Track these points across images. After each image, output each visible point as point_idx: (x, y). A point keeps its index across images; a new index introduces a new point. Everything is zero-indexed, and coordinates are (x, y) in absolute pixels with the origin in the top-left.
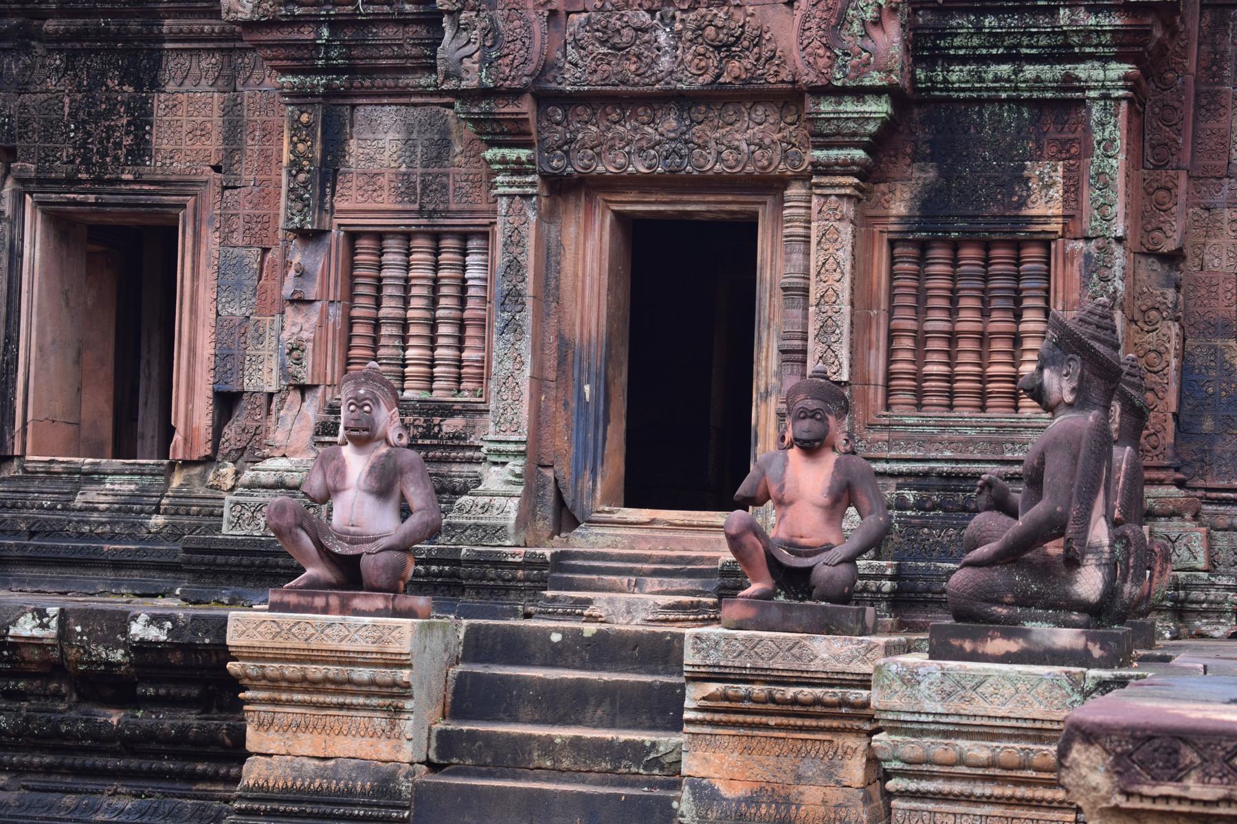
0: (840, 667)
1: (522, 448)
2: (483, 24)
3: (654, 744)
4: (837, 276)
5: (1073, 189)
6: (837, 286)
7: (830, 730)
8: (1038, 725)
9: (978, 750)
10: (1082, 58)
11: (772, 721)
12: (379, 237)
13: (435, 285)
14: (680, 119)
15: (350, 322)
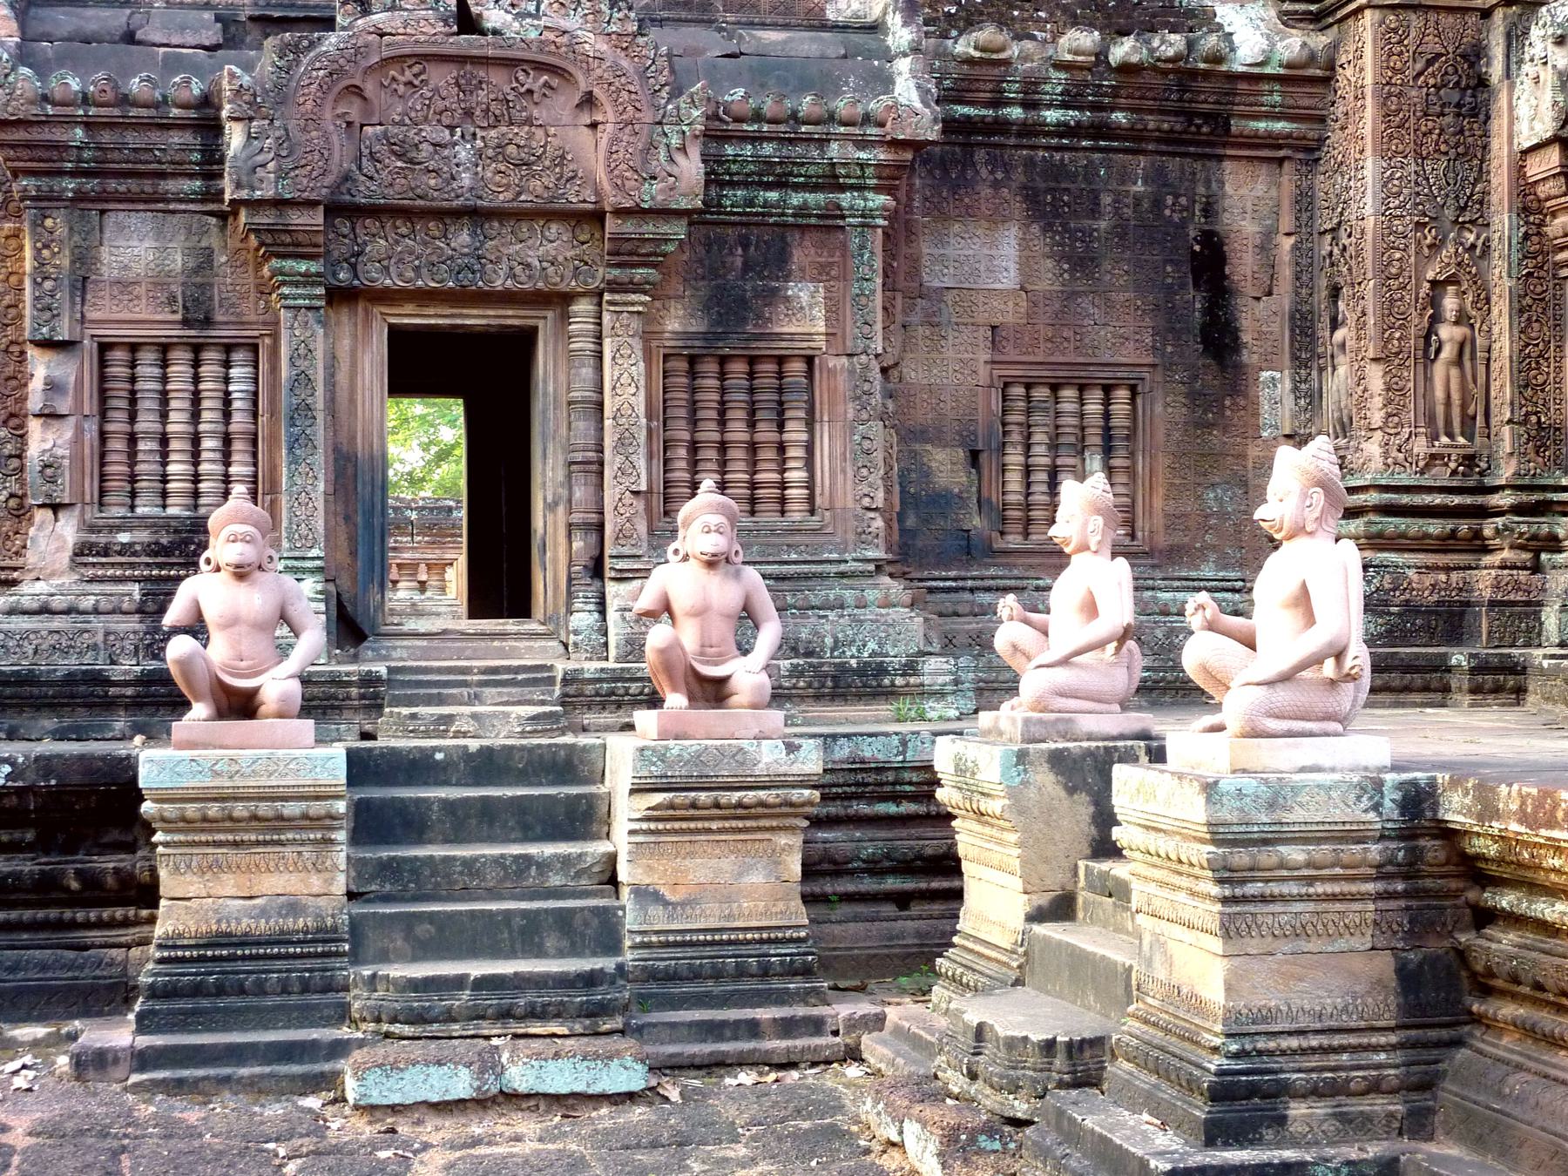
0: (782, 770)
1: (318, 563)
2: (278, 134)
3: (580, 855)
4: (633, 390)
5: (833, 312)
6: (633, 400)
7: (772, 829)
8: (1348, 827)
9: (1295, 854)
10: (843, 188)
11: (714, 825)
12: (134, 348)
13: (196, 398)
14: (473, 234)
15: (103, 436)
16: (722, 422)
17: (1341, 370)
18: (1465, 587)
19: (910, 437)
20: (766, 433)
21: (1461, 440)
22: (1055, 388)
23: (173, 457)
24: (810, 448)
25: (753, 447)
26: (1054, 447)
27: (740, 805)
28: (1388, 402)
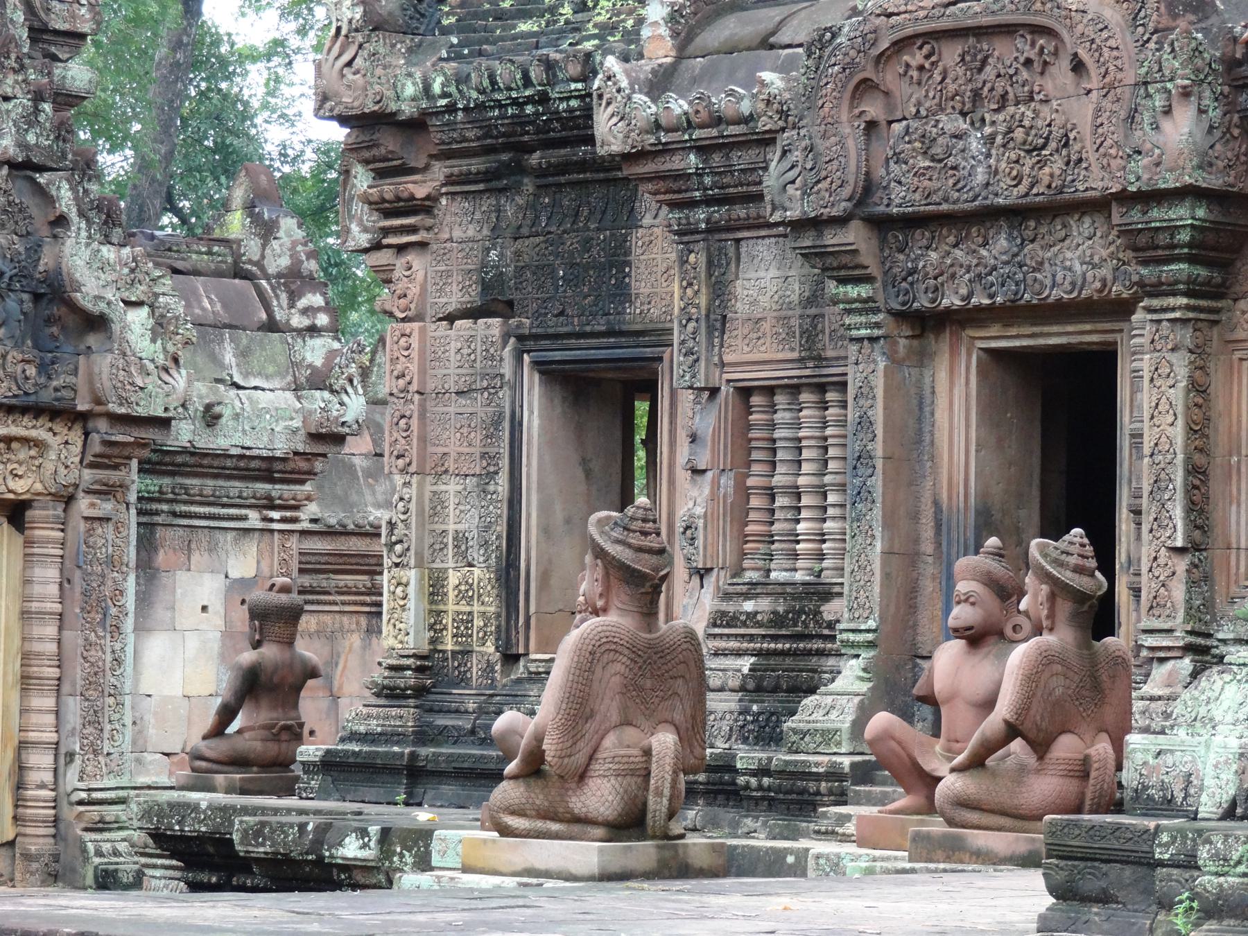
1: (870, 636)
2: (803, 144)
12: (770, 391)
14: (1011, 238)
15: (744, 492)
23: (753, 516)
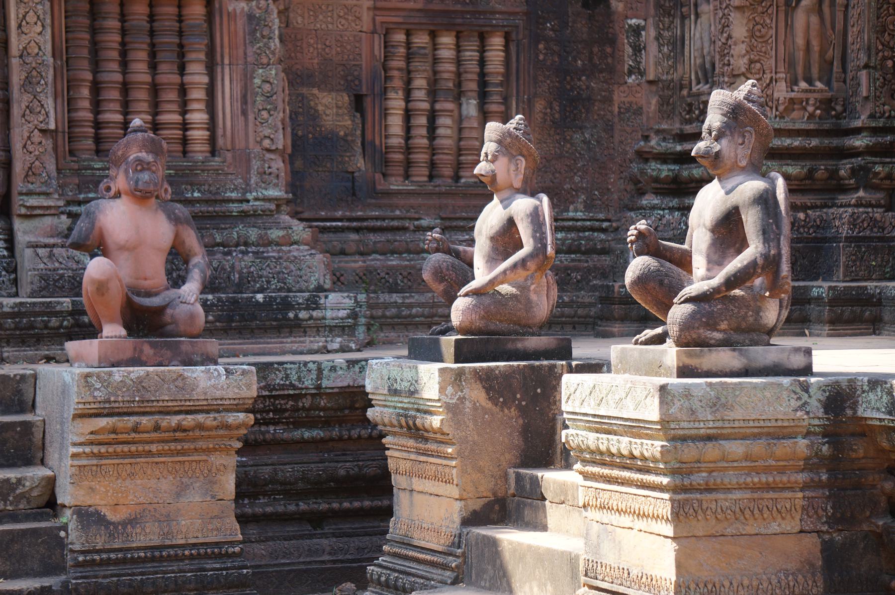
0: (218, 394)
3: (19, 481)
4: (39, 29)
6: (39, 39)
11: (154, 448)
16: (124, 64)
17: (704, 19)
18: (825, 224)
19: (298, 78)
20: (168, 75)
21: (819, 85)
22: (433, 35)
24: (211, 91)
25: (155, 89)
26: (433, 93)
27: (179, 428)
28: (752, 48)
